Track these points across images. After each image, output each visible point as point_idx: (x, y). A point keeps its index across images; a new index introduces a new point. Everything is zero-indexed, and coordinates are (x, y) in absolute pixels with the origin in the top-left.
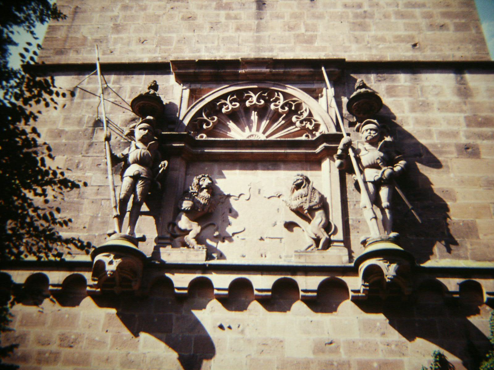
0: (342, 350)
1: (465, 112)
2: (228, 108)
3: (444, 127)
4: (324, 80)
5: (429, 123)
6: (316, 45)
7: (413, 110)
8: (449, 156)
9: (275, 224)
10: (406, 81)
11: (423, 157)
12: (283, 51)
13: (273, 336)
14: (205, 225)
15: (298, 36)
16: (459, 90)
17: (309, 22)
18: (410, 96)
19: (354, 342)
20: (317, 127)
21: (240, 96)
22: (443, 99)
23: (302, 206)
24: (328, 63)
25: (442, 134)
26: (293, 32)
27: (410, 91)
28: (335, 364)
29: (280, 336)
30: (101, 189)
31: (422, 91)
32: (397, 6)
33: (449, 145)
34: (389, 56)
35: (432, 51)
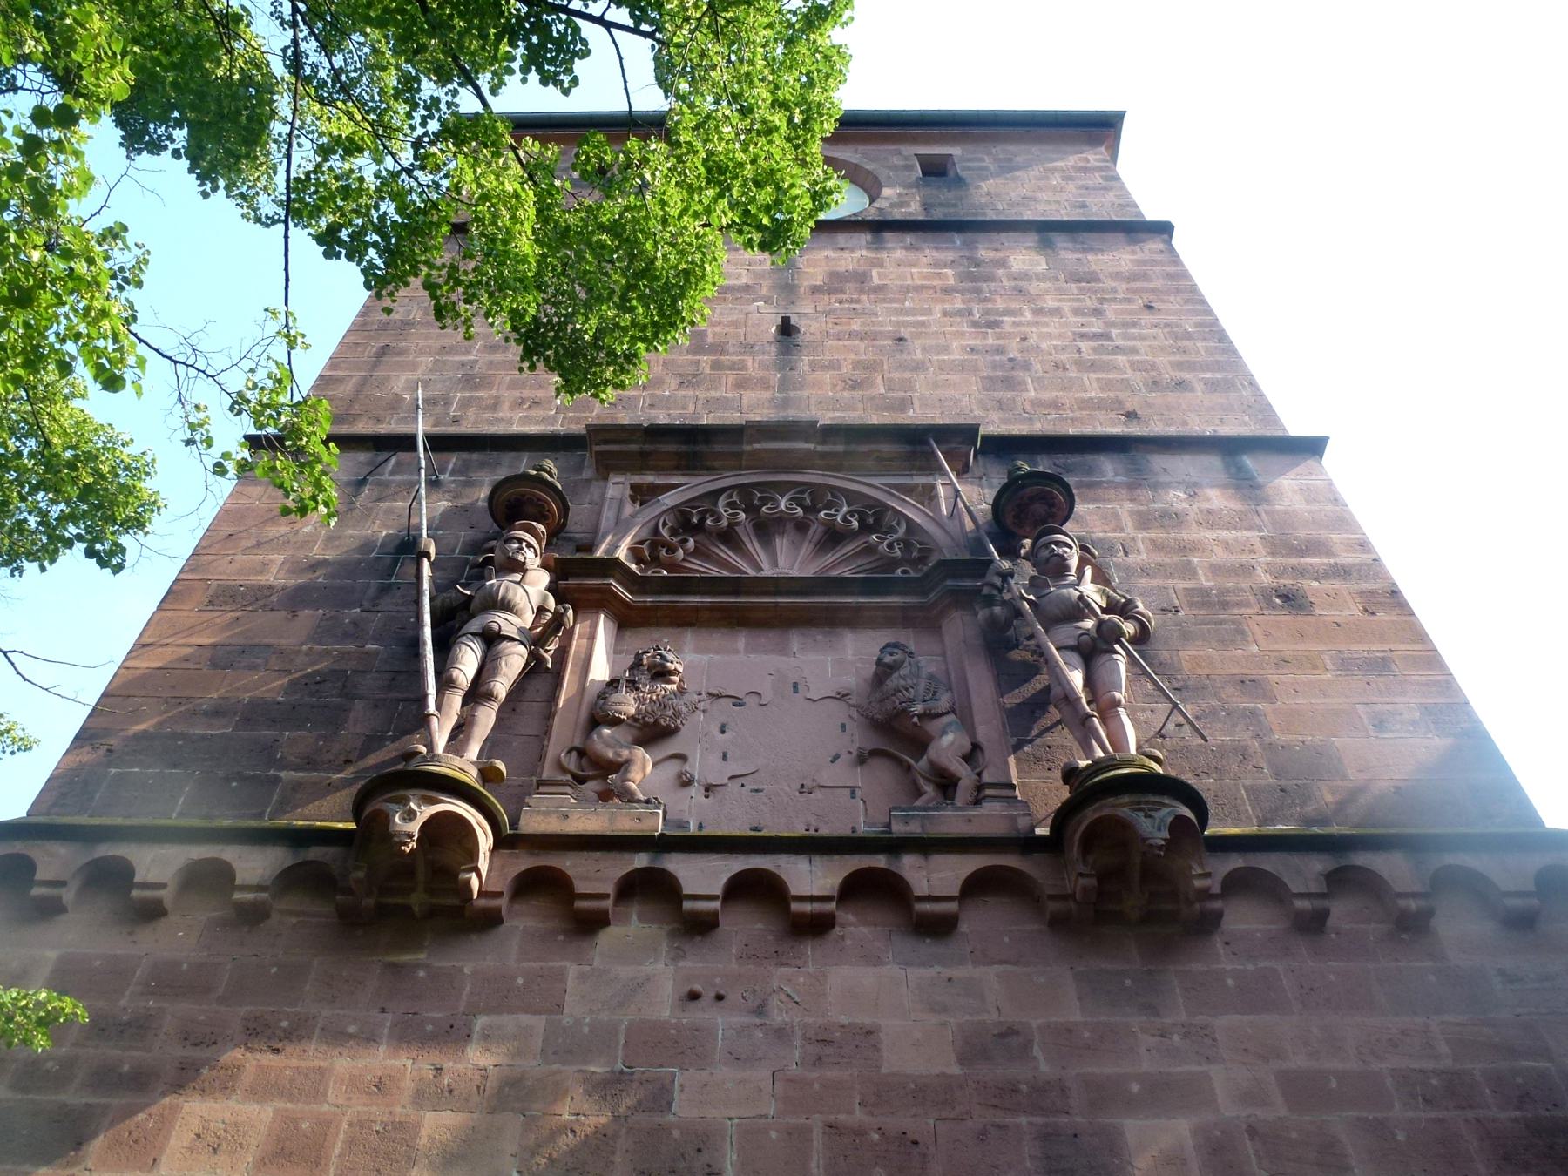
0: (1036, 1051)
1: (1260, 529)
2: (718, 519)
3: (1220, 556)
5: (1184, 548)
8: (1243, 611)
9: (836, 758)
11: (1182, 613)
13: (844, 1020)
14: (661, 756)
15: (873, 398)
17: (896, 375)
19: (1070, 1031)
20: (925, 554)
21: (747, 497)
23: (904, 710)
24: (944, 434)
25: (1216, 570)
26: (858, 394)
28: (1024, 1088)
29: (867, 1020)
30: (401, 677)
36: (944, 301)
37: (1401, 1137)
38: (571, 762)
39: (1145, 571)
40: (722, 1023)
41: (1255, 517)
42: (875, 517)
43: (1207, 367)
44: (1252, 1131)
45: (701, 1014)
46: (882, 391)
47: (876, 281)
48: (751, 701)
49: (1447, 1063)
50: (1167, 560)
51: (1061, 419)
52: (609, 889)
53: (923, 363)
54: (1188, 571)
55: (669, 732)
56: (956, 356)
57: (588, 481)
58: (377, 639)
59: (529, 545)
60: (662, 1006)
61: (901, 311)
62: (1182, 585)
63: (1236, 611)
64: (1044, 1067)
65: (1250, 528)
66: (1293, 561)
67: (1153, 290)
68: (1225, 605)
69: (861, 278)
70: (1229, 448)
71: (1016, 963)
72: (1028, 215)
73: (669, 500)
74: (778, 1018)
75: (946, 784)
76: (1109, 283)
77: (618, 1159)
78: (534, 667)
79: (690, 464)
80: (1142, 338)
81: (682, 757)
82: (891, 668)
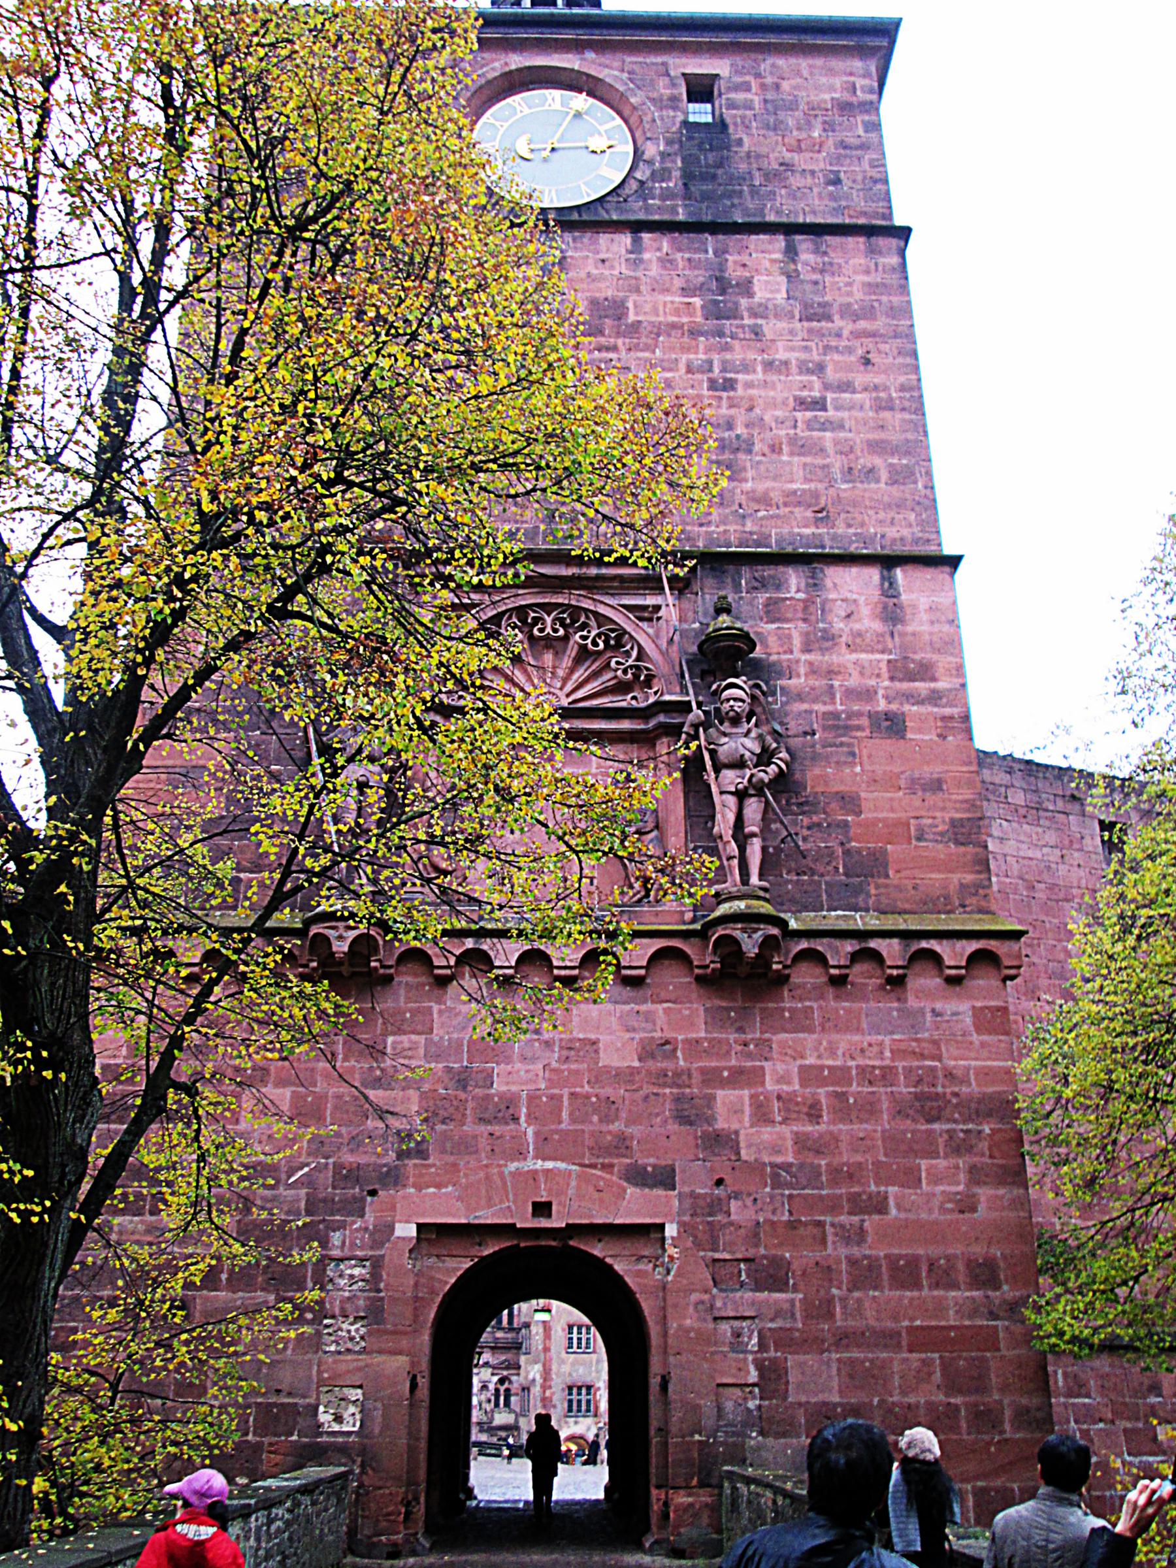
0: (679, 1054)
1: (890, 653)
3: (853, 681)
4: (663, 589)
5: (831, 673)
7: (807, 650)
10: (798, 591)
13: (581, 1036)
16: (885, 608)
18: (805, 620)
22: (857, 626)
25: (849, 693)
27: (805, 608)
29: (593, 1036)
31: (823, 611)
32: (795, 427)
33: (860, 714)
35: (849, 526)
37: (851, 1101)
41: (889, 639)
42: (617, 641)
47: (632, 318)
49: (887, 1062)
62: (819, 708)
64: (682, 1063)
65: (883, 652)
66: (905, 685)
67: (873, 335)
69: (617, 309)
70: (888, 562)
71: (674, 1002)
76: (838, 322)
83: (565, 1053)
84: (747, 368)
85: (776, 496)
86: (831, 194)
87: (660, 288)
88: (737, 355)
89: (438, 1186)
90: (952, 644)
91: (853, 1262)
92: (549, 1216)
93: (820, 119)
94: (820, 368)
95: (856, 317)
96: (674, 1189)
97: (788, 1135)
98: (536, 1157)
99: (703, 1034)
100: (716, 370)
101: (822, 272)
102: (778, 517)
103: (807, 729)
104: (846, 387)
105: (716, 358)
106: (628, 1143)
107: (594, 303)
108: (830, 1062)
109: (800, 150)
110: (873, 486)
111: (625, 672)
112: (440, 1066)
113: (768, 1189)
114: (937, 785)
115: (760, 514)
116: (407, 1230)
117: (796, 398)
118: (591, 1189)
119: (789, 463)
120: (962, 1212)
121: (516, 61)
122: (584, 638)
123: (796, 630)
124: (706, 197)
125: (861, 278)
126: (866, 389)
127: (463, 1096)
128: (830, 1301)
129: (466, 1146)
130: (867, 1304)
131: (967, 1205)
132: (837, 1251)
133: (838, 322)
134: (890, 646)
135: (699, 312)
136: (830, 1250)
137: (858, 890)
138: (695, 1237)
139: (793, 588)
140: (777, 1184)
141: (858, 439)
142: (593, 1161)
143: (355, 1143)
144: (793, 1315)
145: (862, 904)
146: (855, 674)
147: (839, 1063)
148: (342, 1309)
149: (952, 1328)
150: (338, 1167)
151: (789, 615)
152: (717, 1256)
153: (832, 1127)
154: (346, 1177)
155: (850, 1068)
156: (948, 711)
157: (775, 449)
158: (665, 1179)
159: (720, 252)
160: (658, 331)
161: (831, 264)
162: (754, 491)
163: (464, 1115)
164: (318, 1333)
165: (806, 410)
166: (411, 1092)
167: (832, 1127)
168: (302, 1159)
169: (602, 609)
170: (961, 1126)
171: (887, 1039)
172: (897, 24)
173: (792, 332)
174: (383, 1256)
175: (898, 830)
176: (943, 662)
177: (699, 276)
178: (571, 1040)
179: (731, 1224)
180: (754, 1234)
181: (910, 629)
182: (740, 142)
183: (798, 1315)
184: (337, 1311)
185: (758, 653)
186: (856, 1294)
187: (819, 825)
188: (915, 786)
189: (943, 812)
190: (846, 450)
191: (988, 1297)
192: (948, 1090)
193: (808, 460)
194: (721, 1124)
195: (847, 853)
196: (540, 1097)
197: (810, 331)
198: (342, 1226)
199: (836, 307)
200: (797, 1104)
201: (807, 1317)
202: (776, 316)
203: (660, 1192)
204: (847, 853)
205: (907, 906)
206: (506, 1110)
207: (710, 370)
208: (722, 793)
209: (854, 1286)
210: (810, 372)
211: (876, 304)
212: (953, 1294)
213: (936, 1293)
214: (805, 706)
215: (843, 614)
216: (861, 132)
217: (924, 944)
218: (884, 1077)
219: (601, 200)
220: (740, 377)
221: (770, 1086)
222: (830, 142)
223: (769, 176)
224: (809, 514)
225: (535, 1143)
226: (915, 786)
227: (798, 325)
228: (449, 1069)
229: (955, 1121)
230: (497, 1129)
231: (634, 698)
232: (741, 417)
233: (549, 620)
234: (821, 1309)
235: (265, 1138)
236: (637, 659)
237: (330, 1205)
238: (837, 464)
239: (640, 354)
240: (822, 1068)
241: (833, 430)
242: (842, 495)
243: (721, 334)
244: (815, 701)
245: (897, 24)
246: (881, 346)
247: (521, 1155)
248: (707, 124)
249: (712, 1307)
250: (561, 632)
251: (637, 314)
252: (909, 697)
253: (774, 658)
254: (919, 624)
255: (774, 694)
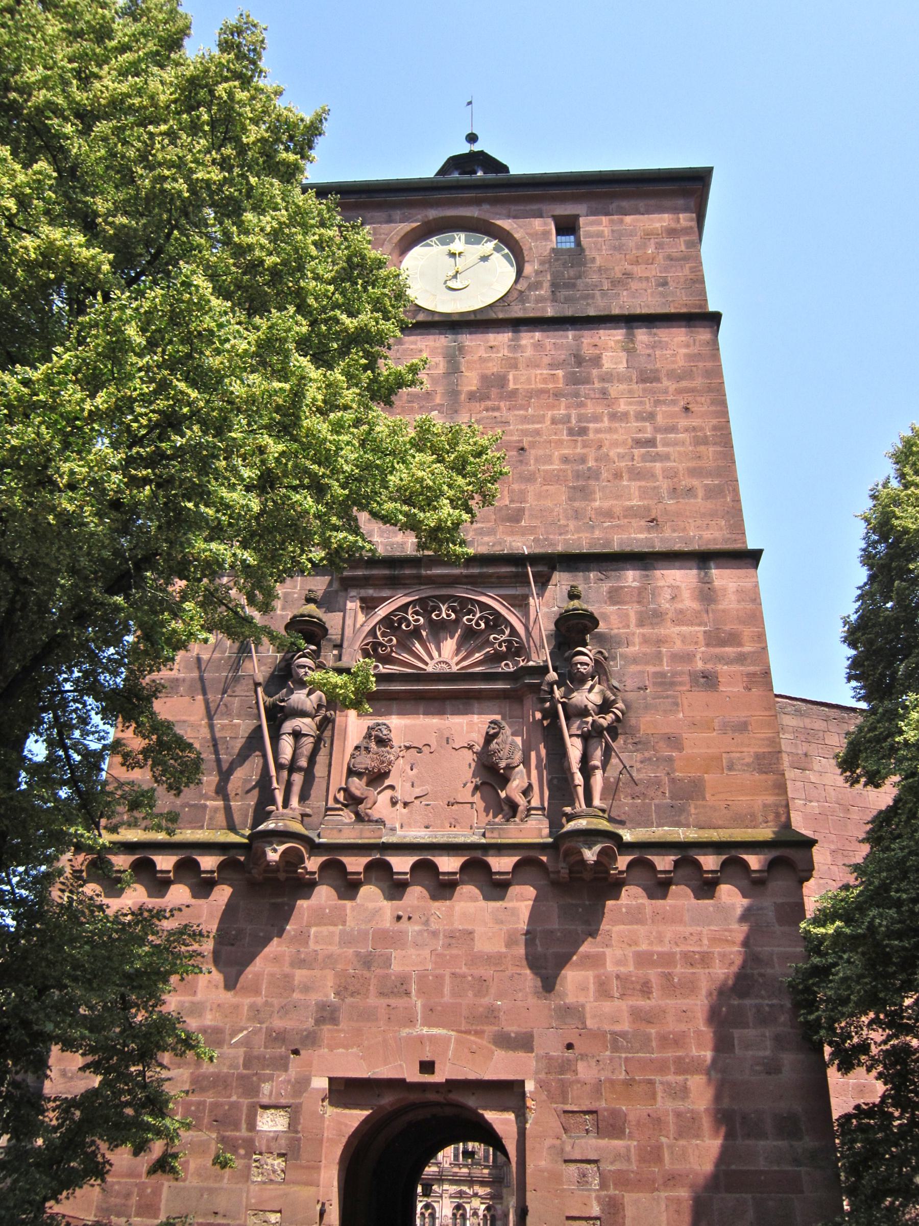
0: (537, 942)
1: (706, 625)
3: (678, 646)
5: (660, 642)
6: (523, 523)
7: (641, 623)
9: (465, 785)
10: (634, 580)
12: (481, 534)
13: (460, 927)
16: (701, 591)
17: (515, 486)
18: (639, 602)
22: (680, 606)
25: (676, 658)
27: (639, 594)
29: (470, 928)
31: (653, 594)
32: (633, 459)
33: (681, 673)
34: (618, 542)
35: (674, 531)
36: (552, 407)
38: (341, 796)
39: (635, 660)
40: (412, 928)
43: (709, 474)
44: (618, 977)
45: (404, 925)
46: (507, 503)
47: (511, 386)
48: (426, 750)
49: (705, 949)
50: (648, 650)
51: (612, 527)
52: (361, 869)
53: (534, 474)
54: (658, 656)
55: (386, 775)
56: (556, 466)
57: (336, 592)
58: (239, 716)
59: (310, 668)
60: (387, 922)
61: (525, 419)
62: (651, 669)
63: (678, 688)
64: (539, 949)
65: (699, 625)
66: (718, 650)
67: (692, 390)
68: (673, 684)
69: (500, 381)
70: (703, 558)
72: (616, 311)
73: (382, 612)
74: (434, 926)
75: (513, 807)
76: (666, 383)
77: (371, 988)
78: (318, 741)
79: (395, 583)
80: (675, 443)
81: (392, 787)
82: (495, 735)
83: (449, 940)
84: (596, 418)
85: (618, 511)
86: (661, 293)
87: (532, 364)
88: (590, 409)
89: (346, 1047)
90: (755, 618)
91: (678, 1115)
92: (433, 1072)
93: (652, 241)
94: (651, 417)
95: (680, 378)
96: (532, 1051)
97: (624, 1008)
98: (423, 1025)
99: (556, 926)
100: (574, 421)
101: (653, 347)
102: (618, 526)
103: (641, 685)
104: (673, 429)
105: (574, 413)
106: (496, 1014)
107: (484, 378)
108: (660, 949)
109: (637, 263)
110: (692, 500)
111: (500, 646)
112: (351, 951)
113: (608, 1053)
114: (743, 727)
115: (606, 525)
116: (320, 1083)
117: (633, 440)
118: (466, 1050)
119: (628, 487)
120: (769, 1073)
121: (433, 214)
122: (470, 620)
123: (632, 610)
124: (568, 300)
125: (684, 351)
126: (686, 430)
127: (366, 974)
128: (659, 1147)
129: (368, 1015)
130: (690, 1151)
131: (772, 1068)
132: (665, 1105)
133: (666, 383)
134: (706, 619)
135: (561, 381)
136: (659, 1103)
137: (682, 810)
138: (549, 1091)
139: (630, 580)
140: (616, 1048)
141: (681, 467)
142: (469, 1027)
143: (284, 1010)
144: (629, 1160)
145: (684, 822)
146: (679, 643)
147: (665, 949)
148: (268, 1147)
149: (762, 1172)
150: (269, 1031)
151: (627, 599)
152: (569, 1107)
153: (660, 1002)
154: (276, 1039)
155: (674, 954)
156: (752, 669)
157: (618, 476)
158: (524, 1043)
159: (575, 338)
160: (532, 394)
161: (660, 342)
162: (601, 508)
163: (368, 990)
164: (249, 1167)
165: (642, 447)
166: (328, 971)
167: (660, 1002)
168: (242, 1024)
169: (483, 599)
170: (767, 1002)
171: (705, 930)
172: (708, 171)
173: (630, 391)
174: (301, 1104)
175: (713, 762)
176: (747, 632)
177: (562, 355)
178: (452, 931)
179: (578, 1081)
180: (597, 1088)
181: (720, 607)
182: (593, 260)
183: (633, 1158)
184: (264, 1149)
185: (602, 628)
186: (682, 1142)
187: (650, 759)
188: (726, 727)
189: (749, 748)
190: (672, 475)
191: (791, 1146)
192: (756, 972)
193: (643, 483)
194: (570, 999)
195: (673, 781)
196: (427, 976)
197: (644, 390)
198: (270, 1078)
199: (664, 372)
200: (632, 982)
201: (642, 1160)
202: (618, 381)
203: (521, 1054)
204: (673, 781)
205: (720, 822)
206: (400, 988)
207: (569, 421)
208: (571, 736)
209: (680, 1135)
210: (644, 419)
211: (694, 369)
212: (762, 1143)
213: (747, 1142)
214: (639, 668)
215: (669, 597)
216: (683, 248)
217: (733, 853)
218: (702, 960)
219: (491, 306)
220: (591, 425)
221: (610, 967)
222: (661, 256)
223: (615, 283)
224: (643, 523)
225: (423, 1012)
226: (726, 727)
227: (635, 386)
228: (357, 954)
229: (762, 998)
230: (393, 1002)
231: (507, 665)
232: (592, 454)
233: (444, 608)
234: (653, 1155)
235: (215, 1006)
236: (510, 635)
237: (262, 1061)
238: (664, 485)
239: (517, 412)
240: (651, 954)
241: (661, 461)
242: (669, 508)
243: (577, 395)
244: (647, 663)
245: (708, 171)
246: (699, 399)
247: (411, 1022)
248: (569, 250)
249: (562, 1150)
250: (453, 616)
251: (515, 384)
252: (720, 659)
253: (616, 631)
254: (729, 602)
255: (614, 659)
